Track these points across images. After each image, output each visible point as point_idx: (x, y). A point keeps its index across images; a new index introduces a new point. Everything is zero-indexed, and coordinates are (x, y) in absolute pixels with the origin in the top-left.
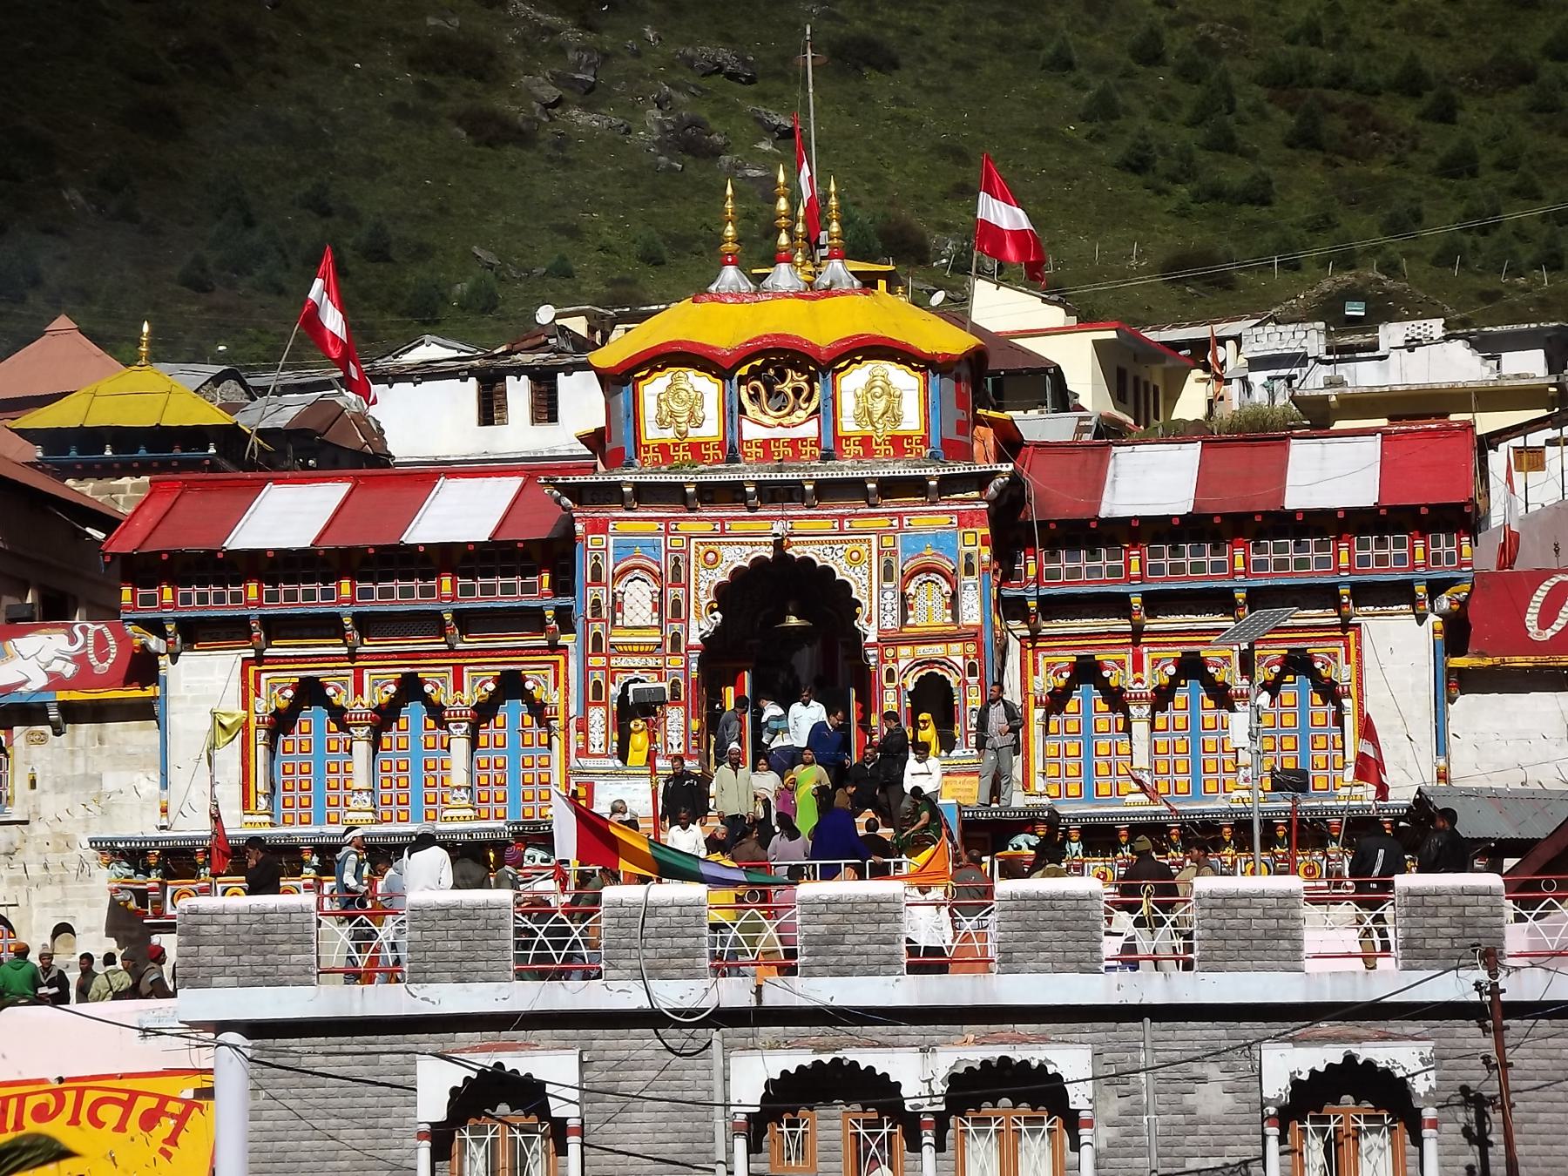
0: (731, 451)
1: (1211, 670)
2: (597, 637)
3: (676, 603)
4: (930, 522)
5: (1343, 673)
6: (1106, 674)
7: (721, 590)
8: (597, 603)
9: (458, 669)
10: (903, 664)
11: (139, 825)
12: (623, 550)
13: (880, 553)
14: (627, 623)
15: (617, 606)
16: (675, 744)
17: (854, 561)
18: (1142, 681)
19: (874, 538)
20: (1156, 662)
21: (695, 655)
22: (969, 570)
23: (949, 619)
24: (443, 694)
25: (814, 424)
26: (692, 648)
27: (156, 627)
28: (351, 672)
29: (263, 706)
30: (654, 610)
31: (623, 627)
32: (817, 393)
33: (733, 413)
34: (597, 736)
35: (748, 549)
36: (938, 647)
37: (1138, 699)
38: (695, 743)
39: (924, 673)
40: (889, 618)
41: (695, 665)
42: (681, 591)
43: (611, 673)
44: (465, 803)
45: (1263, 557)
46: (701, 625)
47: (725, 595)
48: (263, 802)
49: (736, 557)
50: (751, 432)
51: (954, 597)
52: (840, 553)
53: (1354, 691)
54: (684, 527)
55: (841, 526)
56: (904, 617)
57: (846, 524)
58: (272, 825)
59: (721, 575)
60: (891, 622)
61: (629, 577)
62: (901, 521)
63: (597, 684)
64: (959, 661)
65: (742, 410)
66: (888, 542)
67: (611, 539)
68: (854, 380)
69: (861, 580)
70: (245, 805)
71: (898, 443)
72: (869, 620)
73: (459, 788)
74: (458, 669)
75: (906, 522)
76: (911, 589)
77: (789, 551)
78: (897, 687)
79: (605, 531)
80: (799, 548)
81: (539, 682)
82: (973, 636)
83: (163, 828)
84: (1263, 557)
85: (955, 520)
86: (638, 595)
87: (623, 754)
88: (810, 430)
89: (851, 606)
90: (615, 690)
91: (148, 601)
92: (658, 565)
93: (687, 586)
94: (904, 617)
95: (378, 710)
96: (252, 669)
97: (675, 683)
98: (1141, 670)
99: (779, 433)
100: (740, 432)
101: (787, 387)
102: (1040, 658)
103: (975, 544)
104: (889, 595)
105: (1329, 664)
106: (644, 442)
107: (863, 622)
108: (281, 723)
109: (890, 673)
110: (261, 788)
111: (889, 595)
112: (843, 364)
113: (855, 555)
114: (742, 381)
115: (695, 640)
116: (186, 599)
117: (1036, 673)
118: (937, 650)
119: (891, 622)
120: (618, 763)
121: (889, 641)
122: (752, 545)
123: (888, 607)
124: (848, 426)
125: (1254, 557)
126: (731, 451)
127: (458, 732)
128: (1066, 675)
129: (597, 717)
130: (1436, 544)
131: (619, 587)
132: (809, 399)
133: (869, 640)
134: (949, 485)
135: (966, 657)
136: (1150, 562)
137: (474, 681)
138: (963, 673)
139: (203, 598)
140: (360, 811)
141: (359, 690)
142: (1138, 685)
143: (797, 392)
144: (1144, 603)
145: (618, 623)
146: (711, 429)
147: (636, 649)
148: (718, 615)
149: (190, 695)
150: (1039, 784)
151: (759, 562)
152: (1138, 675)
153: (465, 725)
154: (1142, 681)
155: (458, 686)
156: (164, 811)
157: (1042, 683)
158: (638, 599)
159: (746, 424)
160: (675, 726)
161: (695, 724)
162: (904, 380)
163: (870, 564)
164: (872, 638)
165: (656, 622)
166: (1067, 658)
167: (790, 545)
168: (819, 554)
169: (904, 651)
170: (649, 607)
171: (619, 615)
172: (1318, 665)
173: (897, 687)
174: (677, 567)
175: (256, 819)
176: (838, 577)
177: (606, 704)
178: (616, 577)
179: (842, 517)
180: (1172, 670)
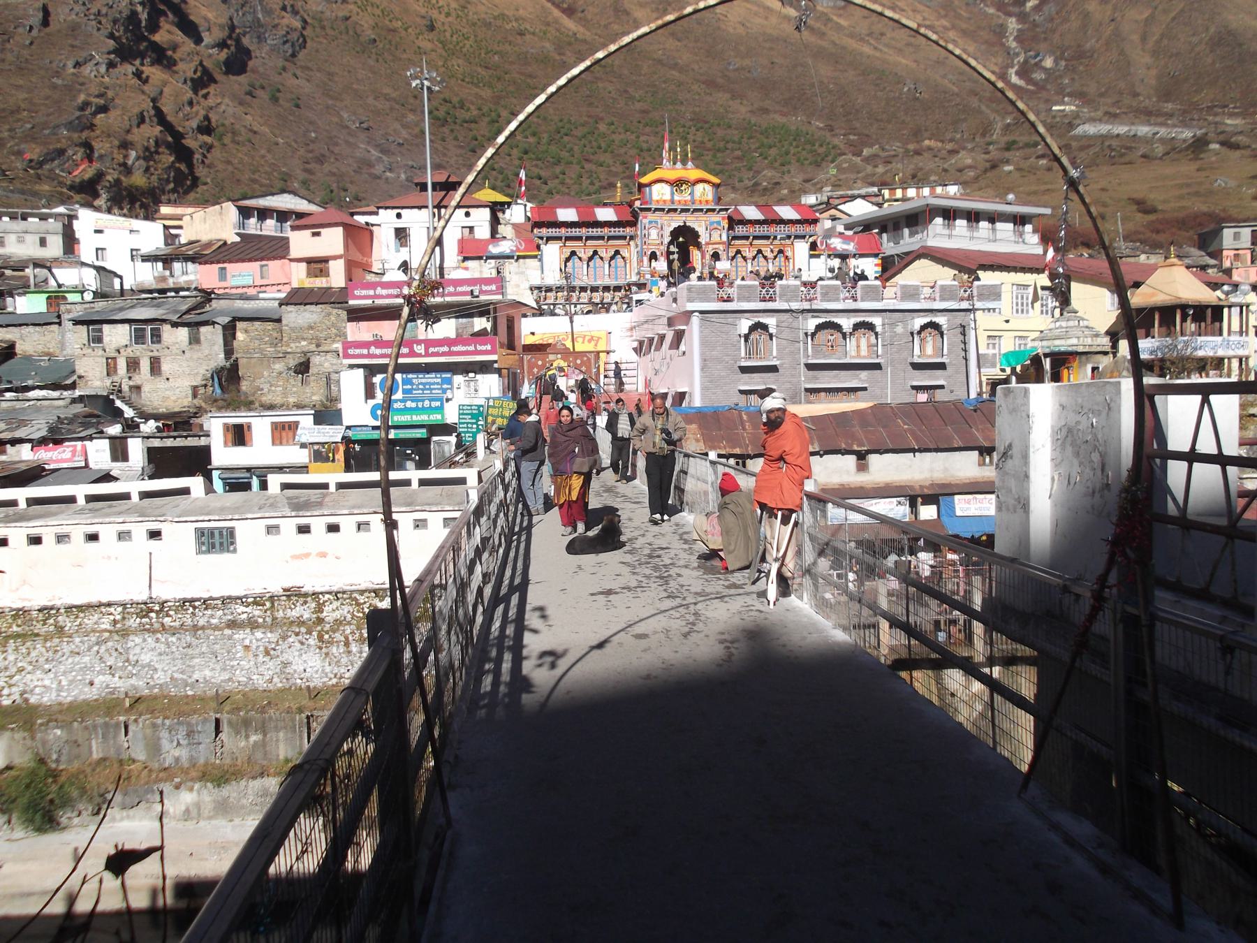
0: (672, 202)
4: (715, 218)
5: (789, 254)
11: (537, 282)
12: (650, 222)
24: (603, 255)
27: (541, 238)
33: (672, 194)
47: (672, 233)
49: (675, 225)
50: (676, 198)
71: (707, 202)
81: (625, 253)
82: (723, 243)
89: (698, 236)
103: (725, 224)
108: (568, 260)
121: (707, 244)
126: (672, 202)
134: (721, 210)
146: (668, 197)
158: (654, 234)
162: (707, 186)
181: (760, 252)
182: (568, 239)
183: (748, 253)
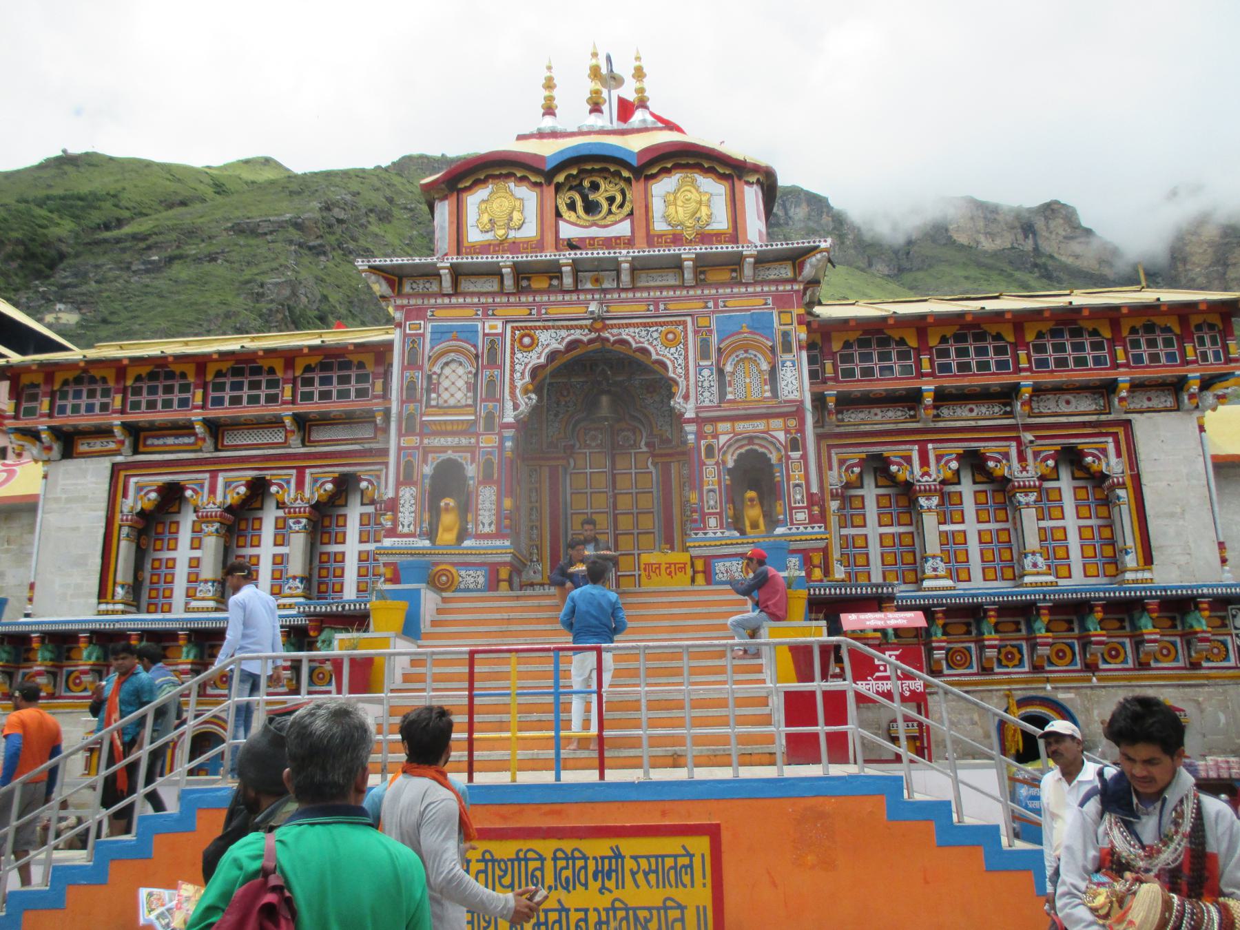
1: (991, 464)
2: (411, 417)
3: (491, 383)
5: (1114, 465)
6: (894, 468)
7: (535, 372)
8: (411, 386)
9: (301, 471)
10: (723, 439)
12: (439, 334)
13: (696, 332)
14: (441, 402)
15: (432, 387)
16: (486, 521)
17: (668, 343)
18: (930, 476)
19: (689, 319)
20: (939, 458)
21: (509, 433)
22: (787, 348)
23: (768, 394)
24: (290, 494)
25: (628, 222)
26: (508, 426)
28: (207, 475)
29: (130, 504)
30: (468, 390)
31: (437, 406)
32: (628, 196)
34: (406, 516)
35: (563, 333)
36: (756, 423)
37: (928, 493)
38: (507, 522)
39: (743, 450)
40: (706, 394)
41: (509, 444)
42: (497, 372)
43: (426, 451)
44: (299, 591)
45: (1043, 356)
46: (515, 405)
48: (119, 590)
49: (550, 340)
51: (773, 372)
52: (655, 335)
53: (1129, 483)
54: (499, 311)
55: (657, 309)
56: (722, 394)
57: (662, 307)
58: (123, 612)
59: (537, 358)
60: (709, 398)
61: (444, 360)
62: (716, 305)
63: (409, 465)
64: (781, 436)
65: (558, 215)
66: (703, 322)
67: (429, 326)
68: (662, 187)
69: (678, 359)
70: (102, 594)
72: (686, 397)
73: (294, 578)
74: (301, 471)
75: (721, 304)
76: (729, 368)
77: (606, 334)
78: (717, 463)
79: (424, 318)
80: (615, 331)
83: (27, 615)
84: (1043, 356)
85: (770, 301)
86: (453, 377)
87: (431, 534)
88: (624, 229)
90: (428, 470)
91: (31, 412)
92: (475, 346)
93: (501, 367)
94: (722, 394)
95: (230, 509)
96: (122, 474)
97: (488, 464)
98: (928, 466)
99: (594, 232)
100: (557, 232)
101: (600, 197)
102: (833, 455)
104: (706, 372)
105: (1099, 459)
106: (465, 244)
107: (681, 400)
109: (710, 449)
110: (120, 579)
111: (706, 372)
112: (654, 171)
113: (671, 336)
114: (558, 187)
115: (509, 418)
116: (62, 410)
117: (831, 469)
118: (760, 425)
119: (709, 398)
120: (427, 543)
122: (568, 328)
123: (706, 384)
124: (659, 226)
125: (1034, 356)
127: (296, 527)
128: (857, 470)
129: (407, 495)
130: (1202, 343)
131: (436, 369)
132: (621, 206)
133: (687, 416)
135: (787, 431)
136: (938, 361)
137: (316, 481)
138: (785, 448)
139: (76, 409)
140: (203, 599)
141: (213, 491)
142: (926, 478)
143: (611, 200)
144: (934, 400)
145: (433, 403)
146: (530, 231)
147: (449, 428)
148: (533, 396)
149: (64, 496)
150: (839, 572)
151: (573, 345)
152: (925, 469)
153: (304, 521)
154: (930, 476)
155: (300, 485)
156: (30, 600)
157: (835, 478)
158: (455, 382)
159: (561, 223)
160: (487, 505)
161: (507, 503)
163: (686, 345)
164: (690, 415)
165: (470, 402)
166: (855, 455)
167: (605, 327)
168: (634, 336)
169: (723, 426)
170: (464, 388)
171: (434, 395)
172: (1089, 459)
173: (717, 463)
174: (492, 351)
175: (110, 607)
176: (654, 357)
177: (414, 484)
178: (433, 360)
179: (656, 303)
180: (954, 465)
181: (975, 462)
182: (137, 434)
183: (925, 469)
